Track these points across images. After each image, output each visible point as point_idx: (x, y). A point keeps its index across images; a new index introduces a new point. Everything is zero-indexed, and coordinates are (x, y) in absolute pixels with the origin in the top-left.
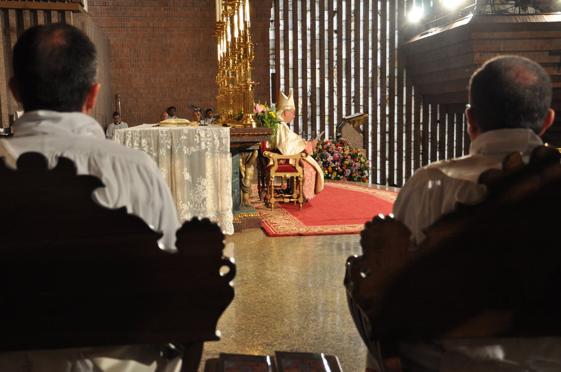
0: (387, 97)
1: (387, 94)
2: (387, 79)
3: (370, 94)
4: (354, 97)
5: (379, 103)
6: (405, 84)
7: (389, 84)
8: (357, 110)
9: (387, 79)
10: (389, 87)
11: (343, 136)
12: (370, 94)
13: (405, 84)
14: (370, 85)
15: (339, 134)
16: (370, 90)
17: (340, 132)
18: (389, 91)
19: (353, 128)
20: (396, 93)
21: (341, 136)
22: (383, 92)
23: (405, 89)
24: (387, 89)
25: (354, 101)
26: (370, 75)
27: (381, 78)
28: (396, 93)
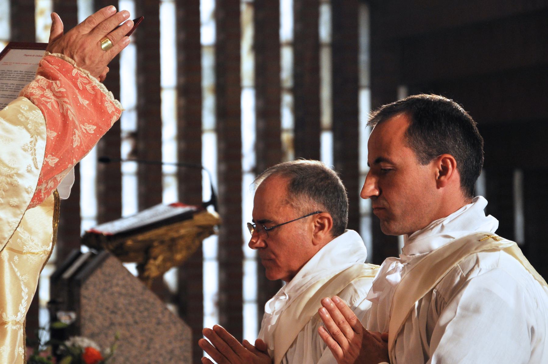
0: (287, 137)
1: (287, 120)
2: (287, 57)
3: (208, 120)
4: (133, 135)
5: (248, 160)
6: (364, 78)
7: (297, 74)
8: (150, 196)
9: (287, 57)
10: (293, 91)
11: (88, 327)
12: (208, 120)
13: (364, 78)
14: (208, 79)
15: (65, 319)
16: (209, 102)
17: (73, 304)
18: (296, 110)
19: (139, 286)
20: (326, 118)
21: (75, 329)
22: (268, 114)
23: (364, 98)
24: (287, 99)
25: (135, 155)
26: (208, 34)
27: (257, 48)
28: (326, 118)
